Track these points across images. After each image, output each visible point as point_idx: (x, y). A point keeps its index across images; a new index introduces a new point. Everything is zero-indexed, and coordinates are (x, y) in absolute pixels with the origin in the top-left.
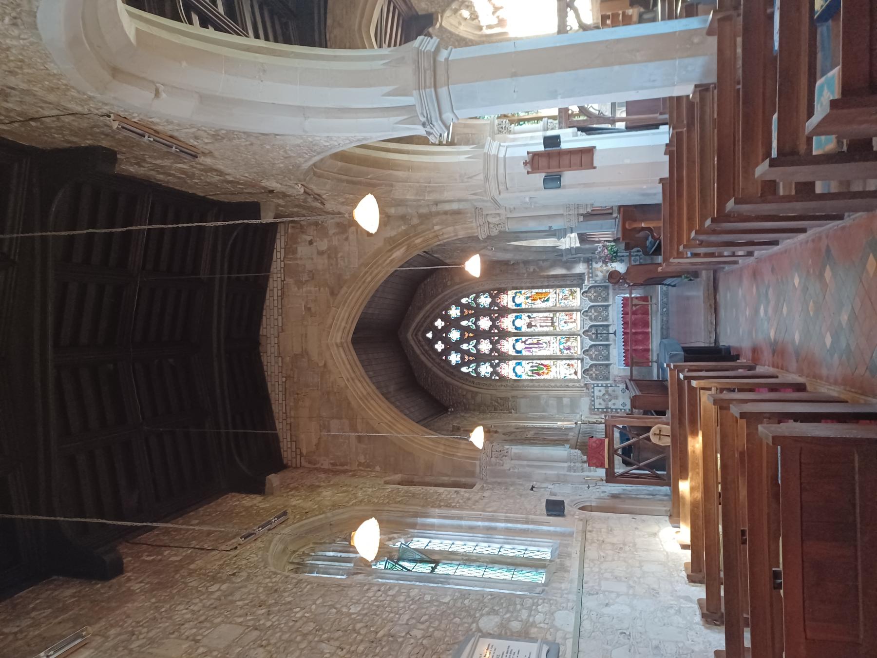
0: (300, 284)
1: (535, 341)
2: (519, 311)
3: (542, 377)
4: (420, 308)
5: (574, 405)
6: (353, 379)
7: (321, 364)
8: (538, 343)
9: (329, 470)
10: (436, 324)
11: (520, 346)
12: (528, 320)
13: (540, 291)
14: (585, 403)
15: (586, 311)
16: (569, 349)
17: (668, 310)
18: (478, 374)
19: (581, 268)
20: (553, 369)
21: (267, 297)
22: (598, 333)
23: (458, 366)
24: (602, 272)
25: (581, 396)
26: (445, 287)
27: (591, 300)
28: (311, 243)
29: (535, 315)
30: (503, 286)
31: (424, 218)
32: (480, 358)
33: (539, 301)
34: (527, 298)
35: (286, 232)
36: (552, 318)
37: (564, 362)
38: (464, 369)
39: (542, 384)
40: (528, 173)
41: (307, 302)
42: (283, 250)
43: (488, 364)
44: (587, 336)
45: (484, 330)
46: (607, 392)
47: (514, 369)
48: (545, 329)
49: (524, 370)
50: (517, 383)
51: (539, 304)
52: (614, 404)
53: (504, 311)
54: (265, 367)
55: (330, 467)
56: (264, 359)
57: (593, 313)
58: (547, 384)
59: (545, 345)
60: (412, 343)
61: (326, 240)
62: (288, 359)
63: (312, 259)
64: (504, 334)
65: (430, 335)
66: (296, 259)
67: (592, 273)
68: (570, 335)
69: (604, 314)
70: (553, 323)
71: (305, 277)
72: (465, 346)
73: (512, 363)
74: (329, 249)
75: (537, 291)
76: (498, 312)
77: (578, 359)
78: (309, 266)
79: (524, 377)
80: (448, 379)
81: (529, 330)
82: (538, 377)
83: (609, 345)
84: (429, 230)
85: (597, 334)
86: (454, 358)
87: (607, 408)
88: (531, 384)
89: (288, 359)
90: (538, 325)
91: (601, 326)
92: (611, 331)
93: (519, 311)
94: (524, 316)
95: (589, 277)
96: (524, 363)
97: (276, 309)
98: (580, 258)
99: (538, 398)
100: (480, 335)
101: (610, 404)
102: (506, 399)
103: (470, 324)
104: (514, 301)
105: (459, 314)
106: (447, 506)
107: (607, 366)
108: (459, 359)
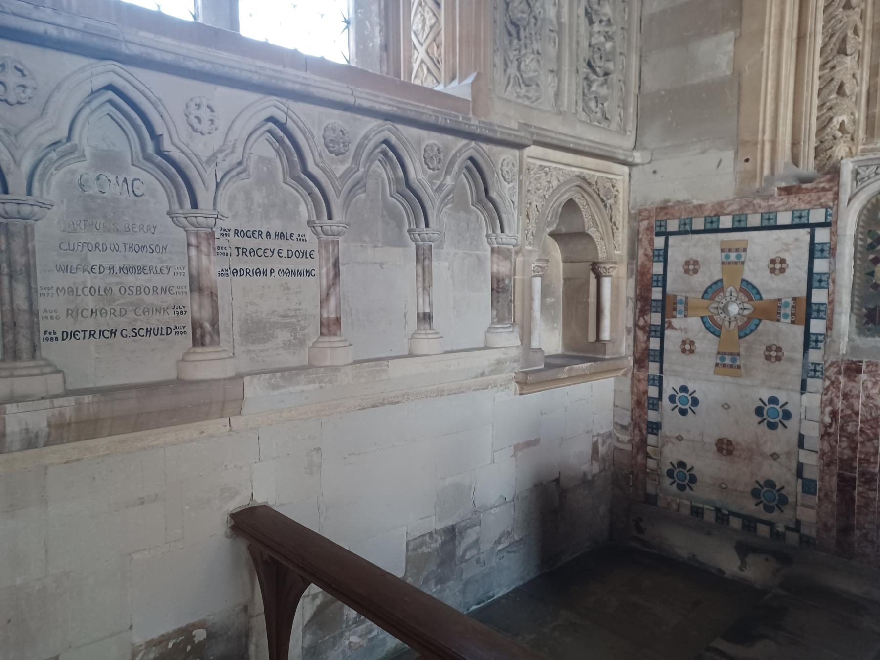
25: (744, 145)
87: (667, 306)
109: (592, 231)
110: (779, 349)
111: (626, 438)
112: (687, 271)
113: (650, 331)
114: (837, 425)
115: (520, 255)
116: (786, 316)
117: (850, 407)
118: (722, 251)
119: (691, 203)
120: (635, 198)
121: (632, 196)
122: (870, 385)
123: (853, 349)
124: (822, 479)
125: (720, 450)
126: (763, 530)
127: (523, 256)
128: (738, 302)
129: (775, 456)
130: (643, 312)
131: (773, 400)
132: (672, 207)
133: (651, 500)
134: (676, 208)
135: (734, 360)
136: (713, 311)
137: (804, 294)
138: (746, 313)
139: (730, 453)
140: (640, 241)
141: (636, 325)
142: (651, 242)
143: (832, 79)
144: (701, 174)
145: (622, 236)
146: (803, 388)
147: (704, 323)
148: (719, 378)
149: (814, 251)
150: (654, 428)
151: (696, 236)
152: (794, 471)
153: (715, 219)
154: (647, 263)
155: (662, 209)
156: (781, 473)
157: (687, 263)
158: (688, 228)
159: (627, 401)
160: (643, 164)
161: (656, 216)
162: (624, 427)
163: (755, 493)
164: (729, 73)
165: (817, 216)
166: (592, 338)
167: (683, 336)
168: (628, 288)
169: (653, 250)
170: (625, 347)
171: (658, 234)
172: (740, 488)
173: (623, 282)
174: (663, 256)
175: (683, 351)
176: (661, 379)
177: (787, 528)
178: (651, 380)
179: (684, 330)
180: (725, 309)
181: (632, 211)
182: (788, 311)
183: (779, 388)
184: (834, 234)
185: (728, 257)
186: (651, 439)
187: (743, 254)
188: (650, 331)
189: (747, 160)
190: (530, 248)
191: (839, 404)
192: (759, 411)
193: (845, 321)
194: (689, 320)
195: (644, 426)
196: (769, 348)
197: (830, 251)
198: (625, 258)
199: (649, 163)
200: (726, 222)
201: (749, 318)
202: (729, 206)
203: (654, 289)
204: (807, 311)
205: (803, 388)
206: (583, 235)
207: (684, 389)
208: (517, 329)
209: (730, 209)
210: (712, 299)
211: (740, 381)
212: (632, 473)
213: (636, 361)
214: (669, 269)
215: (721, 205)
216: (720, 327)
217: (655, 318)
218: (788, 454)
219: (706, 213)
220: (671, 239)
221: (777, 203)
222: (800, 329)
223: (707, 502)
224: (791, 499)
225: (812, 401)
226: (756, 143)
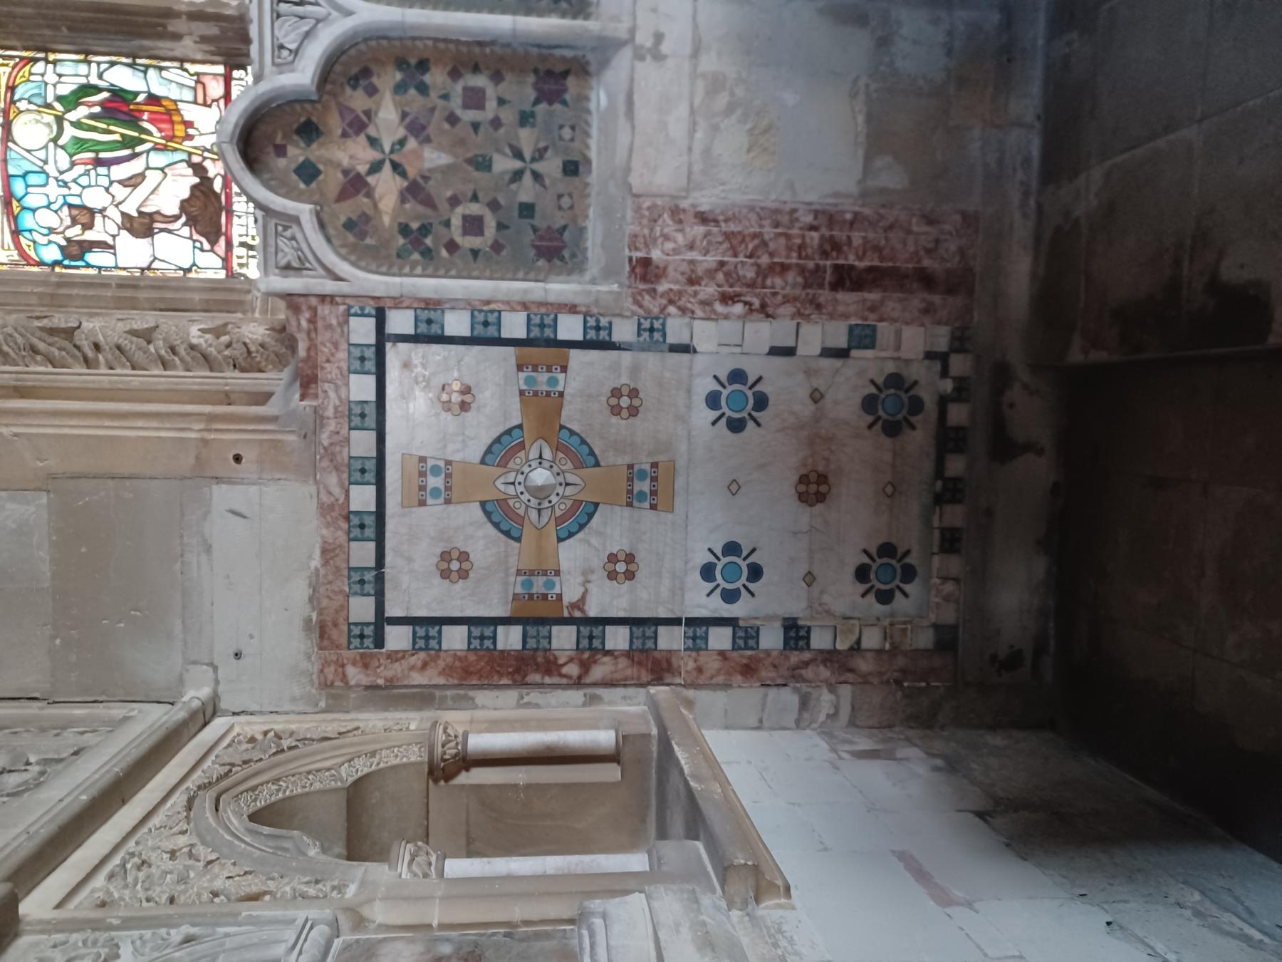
14: (253, 561)
37: (69, 72)
52: (622, 567)
87: (536, 615)
101: (577, 572)
109: (348, 774)
110: (616, 393)
111: (826, 697)
112: (463, 574)
113: (591, 652)
114: (746, 292)
115: (366, 912)
116: (553, 382)
117: (711, 273)
118: (422, 503)
119: (317, 569)
120: (293, 699)
121: (287, 707)
122: (669, 246)
123: (608, 273)
124: (845, 316)
125: (820, 498)
126: (958, 414)
127: (370, 901)
128: (526, 469)
129: (816, 397)
130: (551, 666)
131: (713, 400)
132: (320, 614)
133: (946, 639)
134: (325, 602)
135: (642, 475)
136: (545, 519)
137: (510, 351)
138: (547, 454)
139: (823, 479)
140: (391, 684)
141: (578, 683)
142: (395, 656)
143: (119, 348)
145: (374, 720)
146: (686, 349)
147: (571, 535)
148: (678, 501)
149: (429, 336)
150: (795, 632)
151: (389, 558)
152: (837, 363)
153: (355, 521)
154: (441, 663)
155: (322, 635)
156: (847, 386)
157: (445, 574)
158: (369, 576)
159: (747, 696)
160: (217, 682)
161: (338, 647)
162: (804, 704)
163: (892, 429)
164: (44, 499)
165: (363, 330)
166: (611, 773)
167: (599, 577)
168: (497, 701)
169: (415, 650)
170: (630, 707)
171: (379, 642)
172: (888, 457)
173: (479, 714)
174: (427, 627)
175: (630, 575)
176: (691, 622)
177: (944, 373)
178: (697, 644)
179: (587, 573)
180: (541, 493)
181: (322, 704)
182: (543, 377)
183: (689, 391)
184: (398, 303)
185: (436, 492)
186: (820, 640)
187: (430, 463)
188: (591, 652)
189: (238, 459)
190: (351, 890)
191: (708, 290)
192: (736, 426)
193: (558, 288)
194: (564, 565)
195: (795, 657)
196: (616, 410)
197: (430, 307)
198: (429, 714)
199: (215, 669)
200: (363, 498)
201: (558, 448)
202: (330, 493)
203: (500, 646)
204: (541, 345)
205: (686, 349)
206: (356, 794)
207: (707, 572)
208: (596, 904)
209: (337, 491)
210: (521, 520)
211: (681, 463)
212: (898, 682)
213: (658, 680)
214: (457, 614)
215: (325, 509)
216: (577, 503)
217: (564, 639)
218: (809, 373)
219: (342, 538)
220: (392, 611)
221: (331, 400)
222: (574, 354)
223: (927, 522)
224: (890, 368)
225: (705, 334)
226: (205, 442)
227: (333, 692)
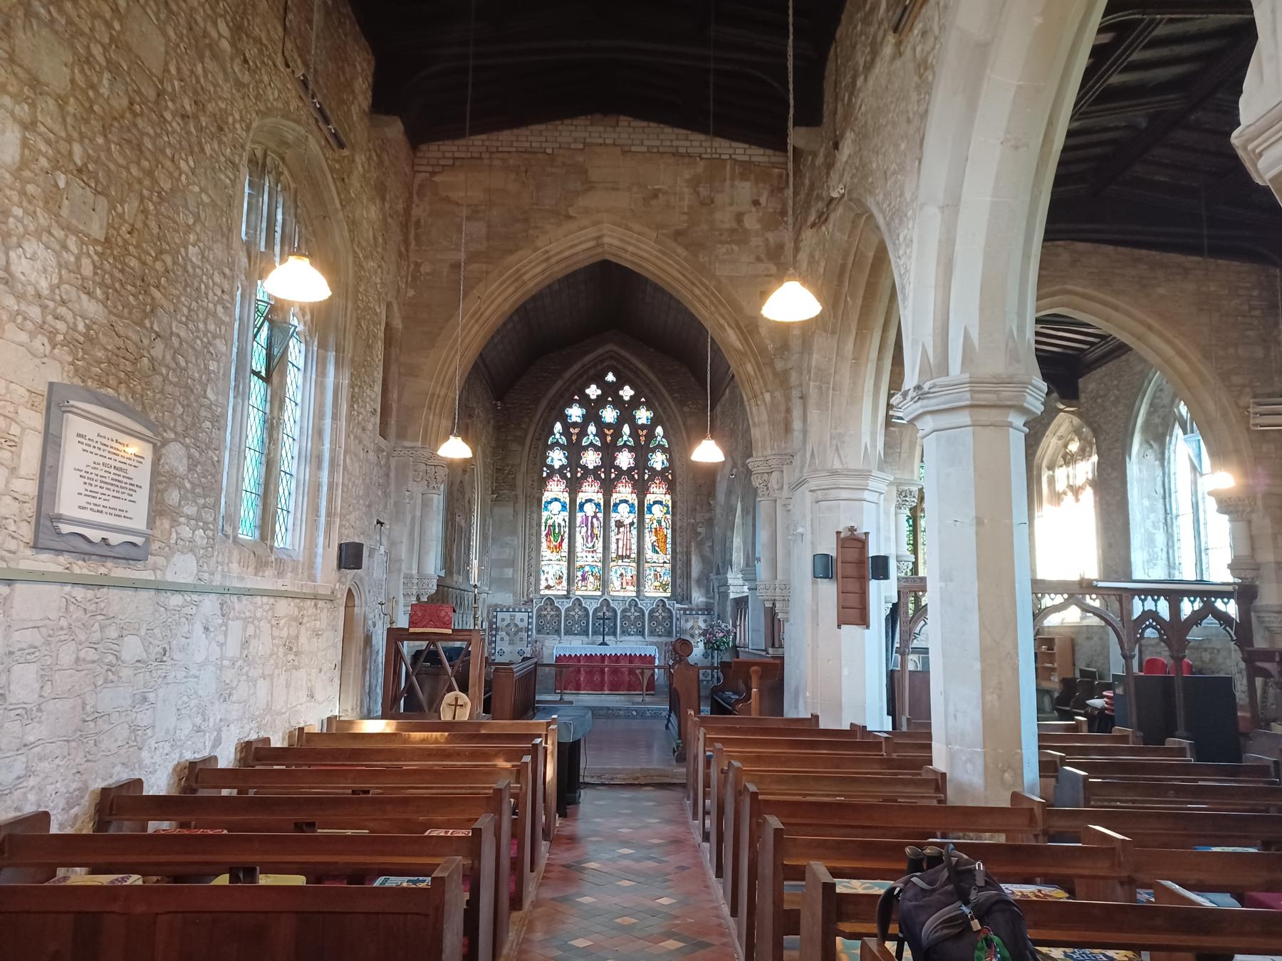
0: (695, 183)
1: (596, 531)
2: (641, 510)
3: (543, 540)
4: (651, 366)
5: (501, 583)
6: (547, 259)
7: (571, 212)
8: (593, 536)
9: (410, 215)
10: (627, 388)
11: (590, 509)
12: (627, 522)
13: (669, 540)
15: (636, 605)
16: (584, 579)
17: (634, 718)
18: (551, 447)
19: (698, 597)
20: (555, 556)
21: (677, 131)
22: (605, 620)
23: (564, 419)
24: (692, 628)
25: (514, 594)
26: (682, 403)
27: (652, 611)
28: (756, 203)
29: (634, 532)
30: (678, 488)
31: (783, 379)
32: (575, 451)
33: (654, 538)
34: (659, 522)
35: (774, 165)
36: (629, 557)
37: (565, 572)
38: (558, 427)
39: (534, 538)
40: (838, 533)
41: (665, 193)
42: (747, 158)
43: (565, 461)
44: (602, 605)
45: (615, 458)
46: (521, 630)
47: (556, 500)
48: (613, 547)
49: (554, 514)
50: (536, 503)
51: (649, 539)
52: (502, 639)
53: (641, 489)
54: (568, 122)
55: (414, 219)
56: (581, 121)
57: (633, 614)
58: (533, 546)
59: (590, 545)
60: (600, 351)
61: (758, 226)
62: (580, 159)
63: (731, 204)
64: (608, 487)
65: (610, 377)
66: (732, 179)
67: (690, 612)
68: (604, 583)
69: (632, 630)
70: (622, 557)
71: (704, 191)
72: (592, 429)
73: (565, 497)
74: (746, 231)
75: (669, 536)
76: (641, 479)
77: (568, 591)
78: (720, 198)
79: (545, 514)
80: (544, 402)
81: (613, 524)
82: (544, 533)
83: (587, 635)
84: (765, 385)
85: (604, 619)
86: (575, 413)
87: (497, 629)
88: (534, 523)
89: (580, 159)
90: (620, 536)
91: (615, 625)
92: (607, 638)
93: (641, 510)
94: (633, 517)
95: (685, 610)
96: (566, 514)
97: (658, 143)
98: (713, 598)
99: (514, 532)
100: (608, 451)
102: (513, 487)
103: (625, 438)
104: (655, 502)
105: (640, 422)
106: (353, 396)
107: (558, 632)
108: (574, 419)
144: (505, 598)
227: (489, 606)
